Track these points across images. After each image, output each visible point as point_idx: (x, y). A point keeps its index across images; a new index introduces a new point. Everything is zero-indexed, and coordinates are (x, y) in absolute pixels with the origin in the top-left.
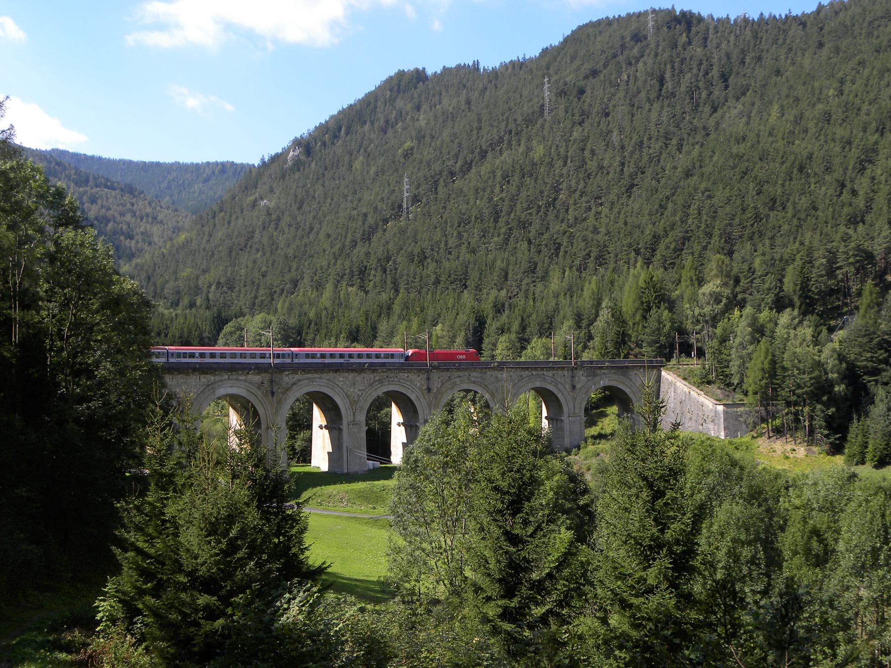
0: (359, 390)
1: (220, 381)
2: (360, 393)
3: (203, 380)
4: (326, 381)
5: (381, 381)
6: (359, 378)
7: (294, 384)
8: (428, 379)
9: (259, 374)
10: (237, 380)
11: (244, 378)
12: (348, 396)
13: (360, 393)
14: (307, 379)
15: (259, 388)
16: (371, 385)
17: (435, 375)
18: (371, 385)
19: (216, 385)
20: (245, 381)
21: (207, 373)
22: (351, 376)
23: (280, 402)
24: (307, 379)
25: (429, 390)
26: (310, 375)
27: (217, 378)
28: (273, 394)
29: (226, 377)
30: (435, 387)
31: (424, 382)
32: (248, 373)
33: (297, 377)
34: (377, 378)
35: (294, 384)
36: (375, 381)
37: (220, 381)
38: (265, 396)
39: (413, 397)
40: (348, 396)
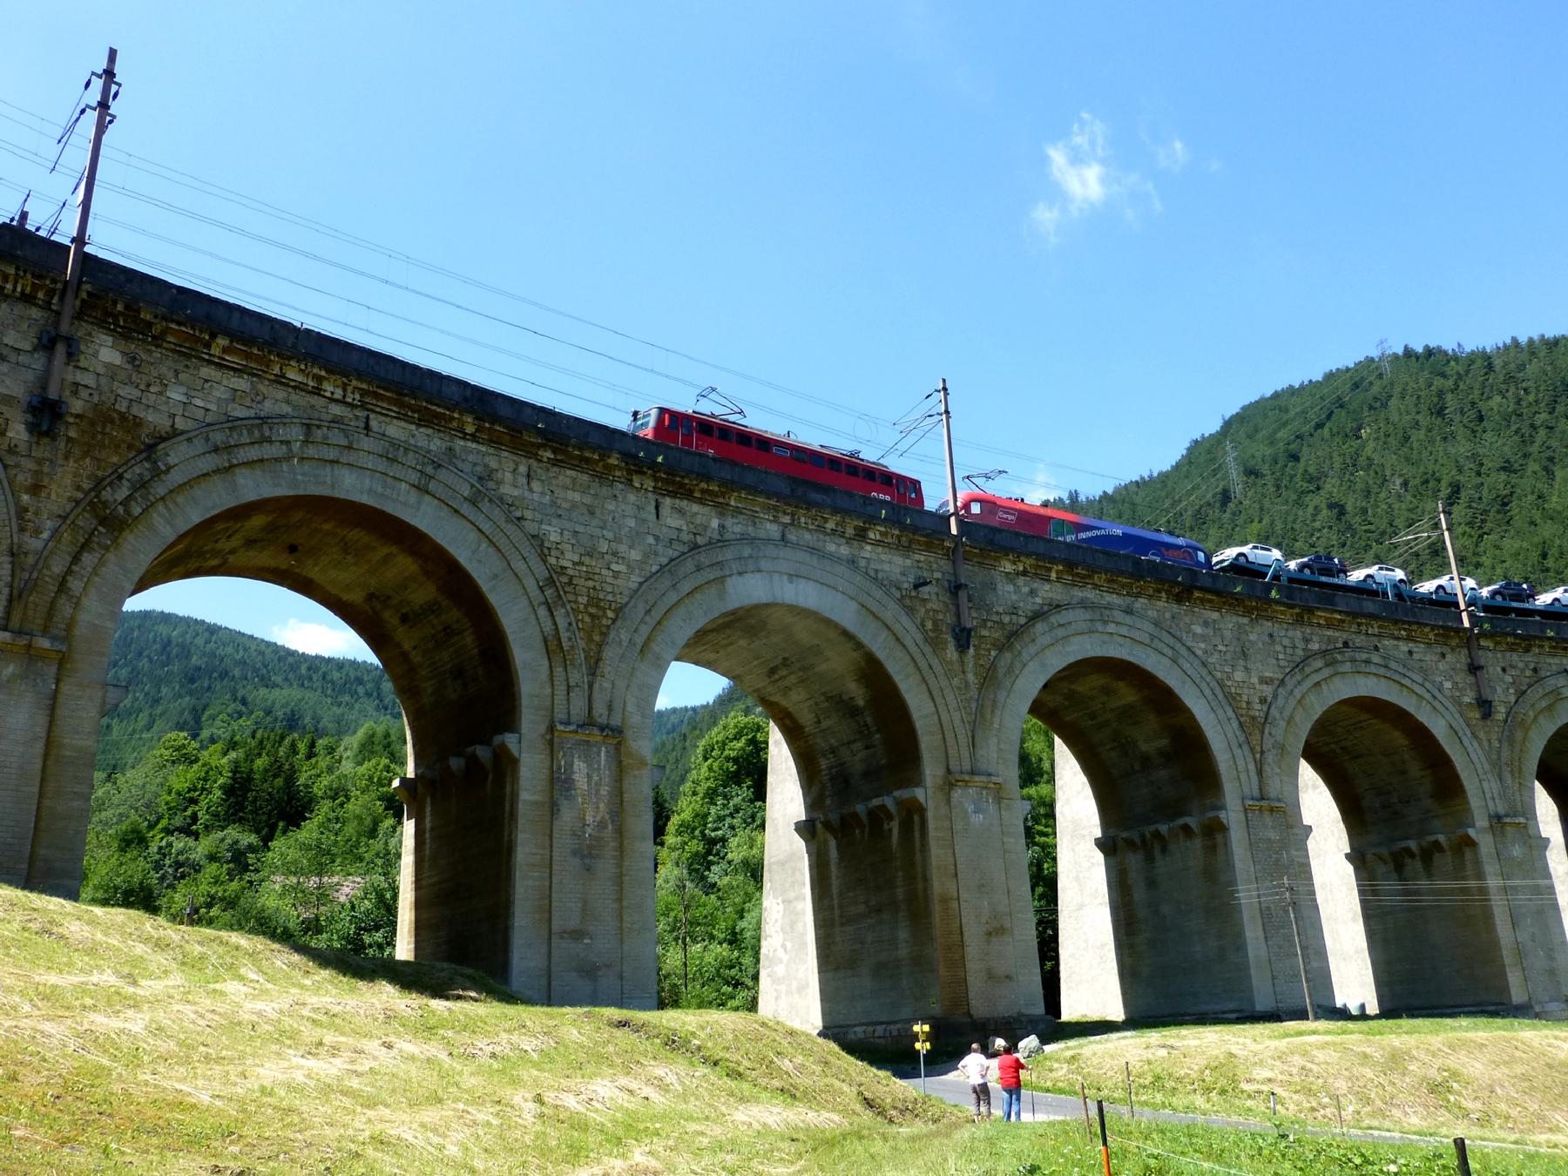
0: (1263, 681)
1: (751, 540)
2: (1268, 690)
3: (673, 521)
4: (1150, 628)
5: (1328, 655)
6: (1256, 634)
7: (1037, 616)
8: (1474, 669)
9: (906, 548)
10: (812, 550)
11: (844, 551)
12: (1231, 699)
13: (1268, 690)
14: (1084, 605)
15: (910, 611)
16: (1299, 665)
17: (1493, 659)
18: (1299, 665)
19: (729, 554)
20: (852, 562)
21: (688, 495)
22: (1230, 622)
23: (989, 678)
24: (1084, 605)
25: (1485, 706)
26: (1090, 594)
27: (735, 526)
28: (963, 638)
29: (773, 529)
30: (1502, 697)
31: (1464, 679)
32: (861, 535)
33: (1048, 592)
34: (1315, 646)
35: (1037, 616)
36: (1309, 656)
37: (745, 539)
38: (935, 643)
39: (1439, 729)
40: (1231, 699)
